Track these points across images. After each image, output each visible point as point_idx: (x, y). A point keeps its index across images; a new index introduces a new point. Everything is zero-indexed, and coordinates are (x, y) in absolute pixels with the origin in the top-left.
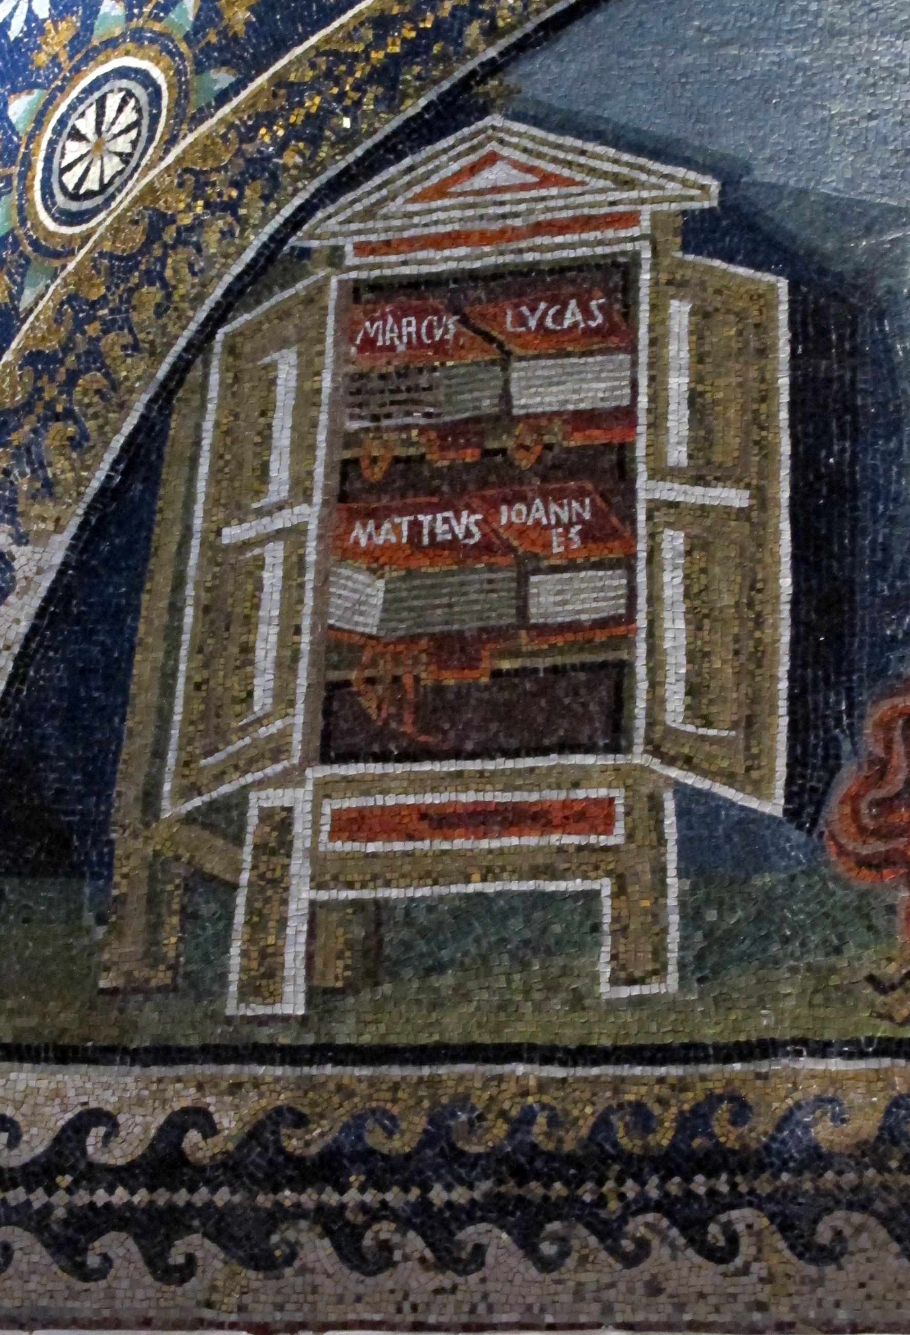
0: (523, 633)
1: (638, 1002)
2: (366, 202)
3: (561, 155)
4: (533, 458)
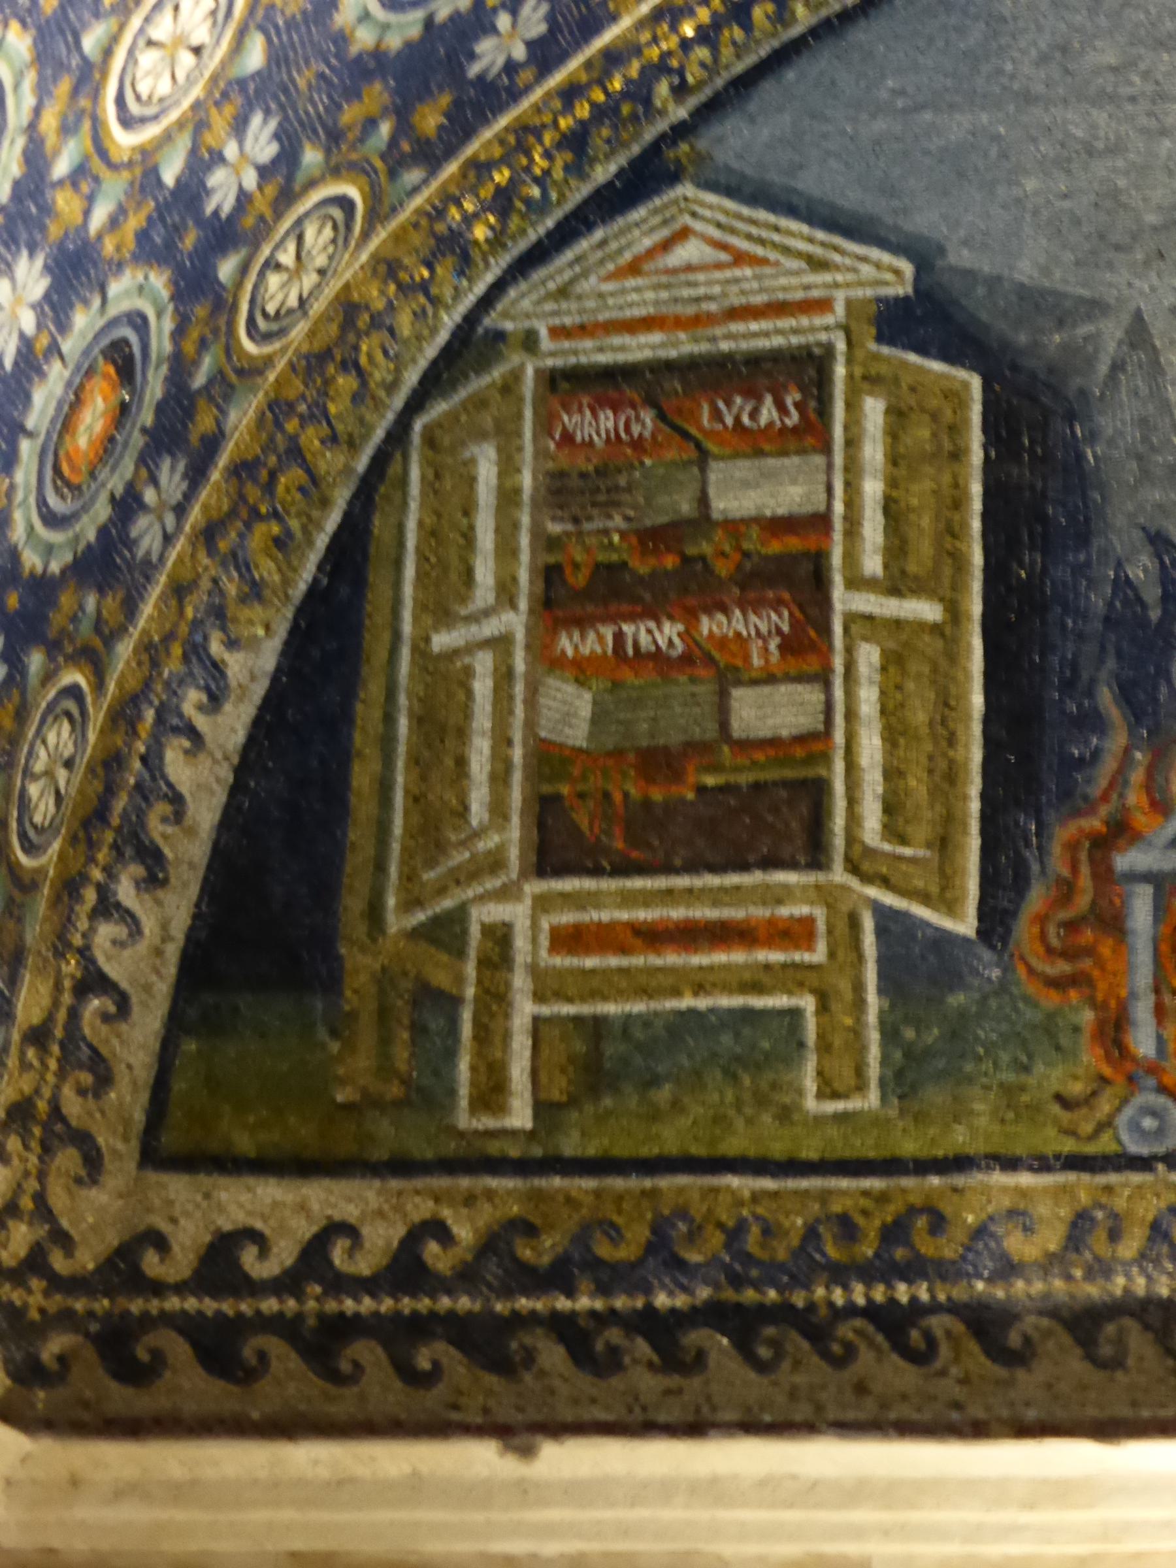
0: (726, 749)
1: (841, 1118)
2: (560, 280)
3: (754, 231)
4: (732, 566)
